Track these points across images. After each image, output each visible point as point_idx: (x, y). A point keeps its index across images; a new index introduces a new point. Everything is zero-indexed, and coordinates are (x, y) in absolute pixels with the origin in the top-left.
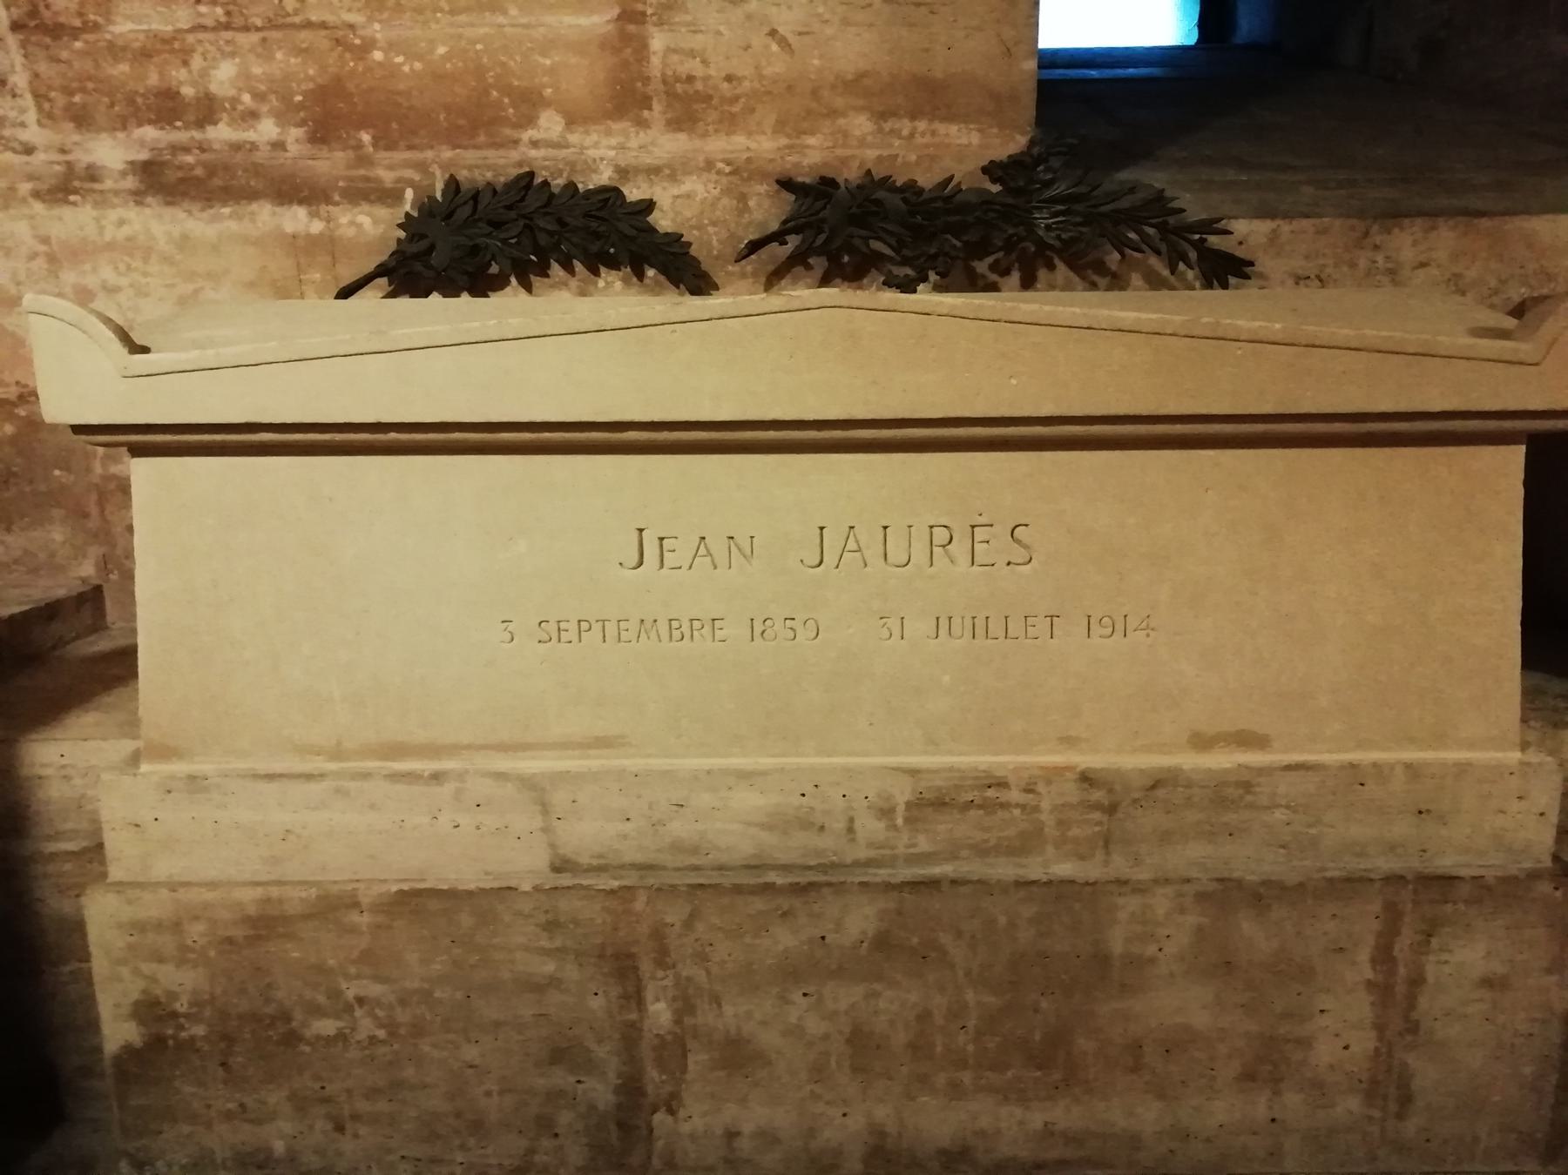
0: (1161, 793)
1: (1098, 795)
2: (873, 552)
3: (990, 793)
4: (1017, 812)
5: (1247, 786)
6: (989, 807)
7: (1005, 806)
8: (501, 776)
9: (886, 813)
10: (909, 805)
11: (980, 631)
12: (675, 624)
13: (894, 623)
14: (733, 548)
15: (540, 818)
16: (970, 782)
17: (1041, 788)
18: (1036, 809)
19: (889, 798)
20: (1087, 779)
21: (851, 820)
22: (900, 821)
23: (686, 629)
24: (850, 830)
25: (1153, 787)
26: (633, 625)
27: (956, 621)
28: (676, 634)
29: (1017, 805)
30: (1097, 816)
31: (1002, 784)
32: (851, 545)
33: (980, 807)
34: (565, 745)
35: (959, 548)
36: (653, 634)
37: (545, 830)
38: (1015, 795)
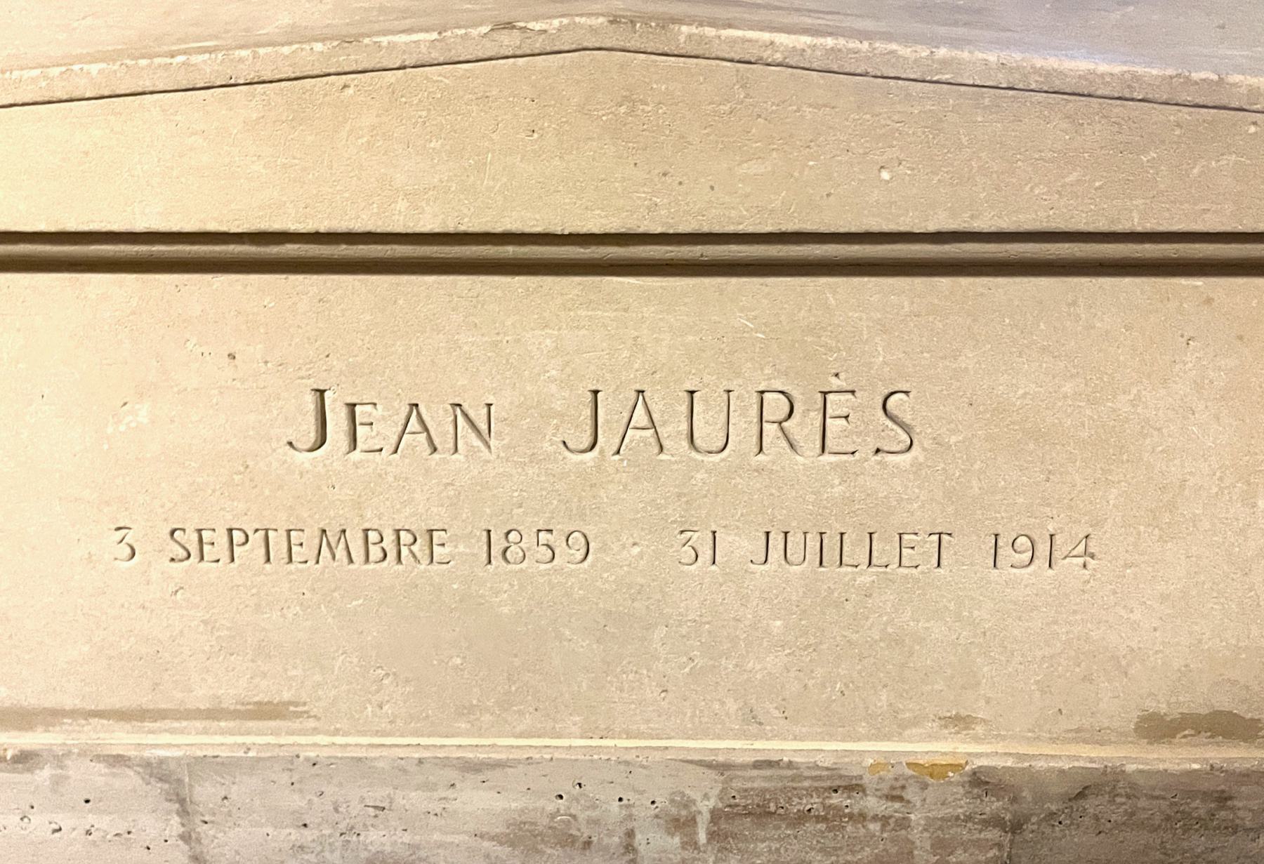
0: (1091, 805)
1: (993, 806)
2: (673, 430)
3: (836, 799)
4: (874, 827)
5: (1223, 799)
6: (833, 818)
7: (862, 817)
8: (118, 761)
9: (681, 823)
10: (715, 815)
11: (831, 554)
12: (373, 536)
13: (702, 540)
14: (460, 419)
15: (175, 820)
16: (806, 784)
17: (911, 794)
18: (904, 823)
19: (687, 803)
20: (981, 782)
21: (630, 834)
22: (702, 837)
23: (389, 543)
24: (629, 848)
25: (1081, 795)
26: (310, 537)
27: (795, 540)
28: (375, 552)
29: (875, 818)
30: (993, 834)
31: (854, 787)
32: (640, 417)
33: (818, 819)
34: (213, 714)
35: (804, 427)
36: (340, 552)
37: (185, 837)
38: (872, 804)
